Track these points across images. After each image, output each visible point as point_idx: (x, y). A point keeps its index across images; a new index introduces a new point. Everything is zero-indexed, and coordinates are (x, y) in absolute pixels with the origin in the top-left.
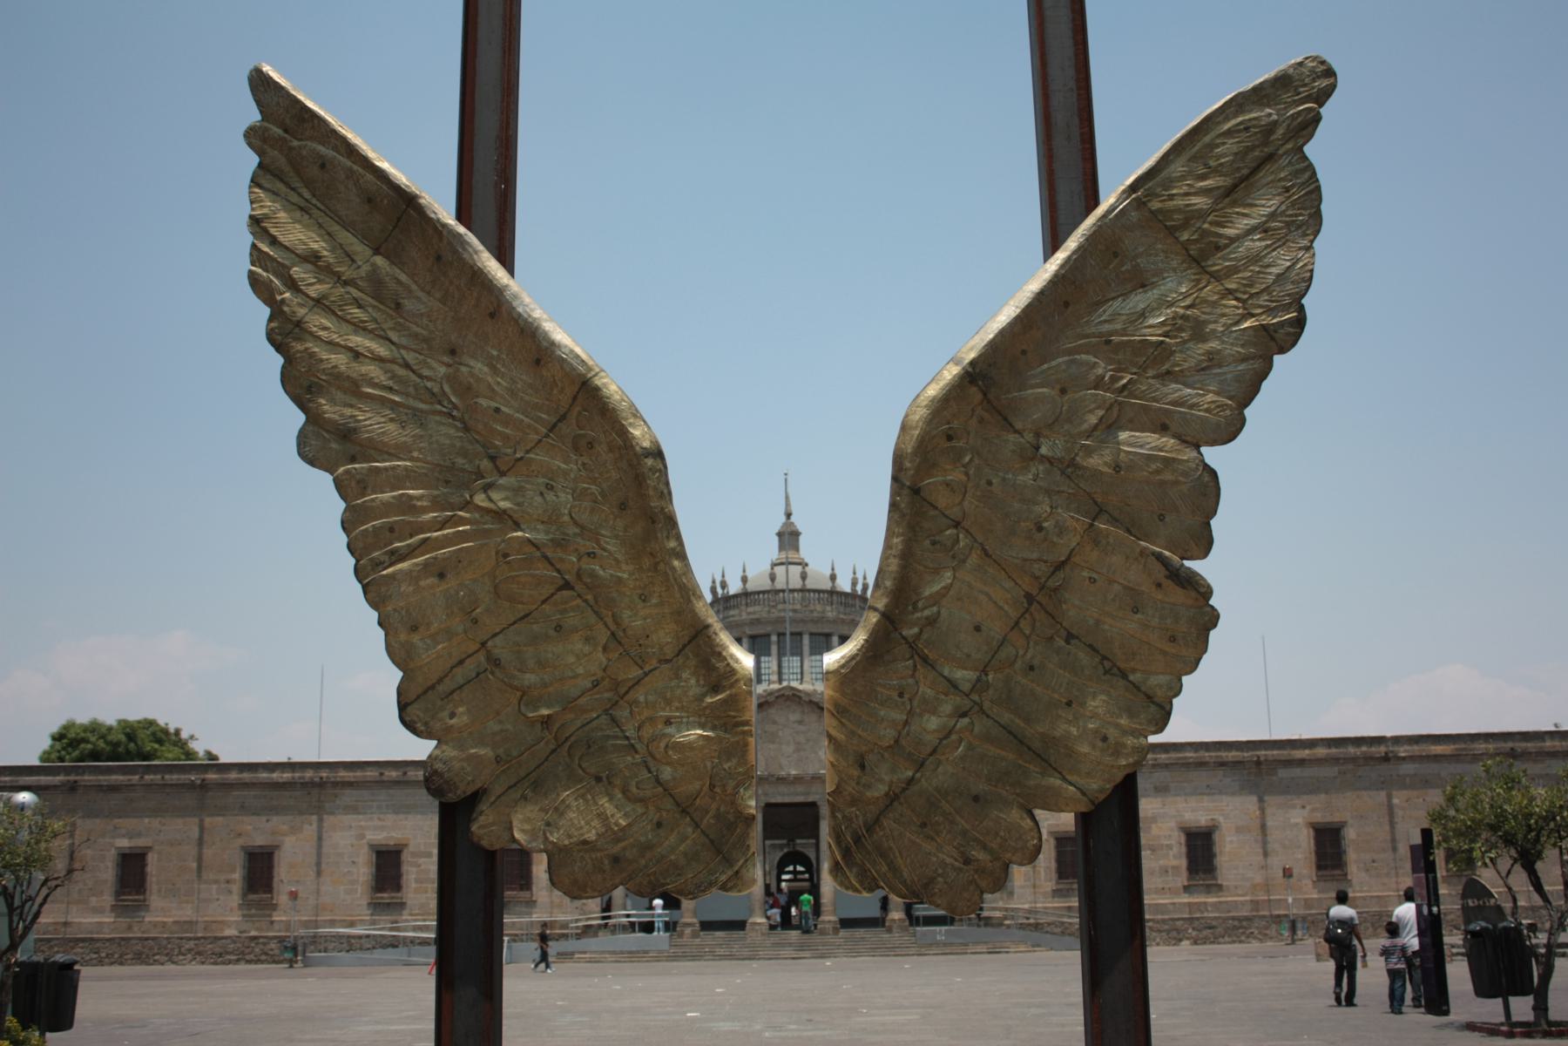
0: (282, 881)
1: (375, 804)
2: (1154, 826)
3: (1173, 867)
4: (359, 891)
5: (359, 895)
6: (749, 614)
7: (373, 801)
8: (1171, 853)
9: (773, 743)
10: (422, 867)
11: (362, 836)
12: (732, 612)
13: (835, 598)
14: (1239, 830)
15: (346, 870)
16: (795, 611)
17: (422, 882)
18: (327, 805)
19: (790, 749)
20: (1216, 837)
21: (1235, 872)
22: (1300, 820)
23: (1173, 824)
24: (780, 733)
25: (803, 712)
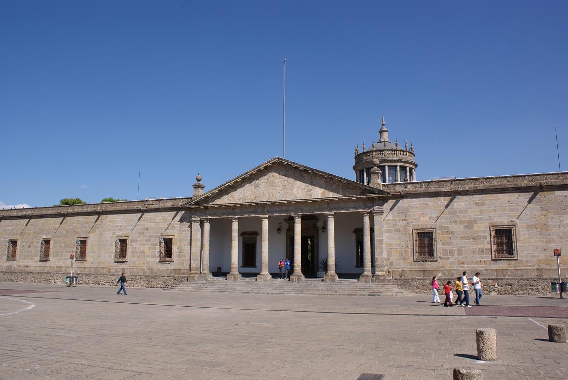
2: (475, 225)
3: (486, 249)
7: (118, 219)
8: (486, 241)
11: (114, 233)
13: (398, 151)
14: (529, 227)
16: (382, 157)
17: (133, 253)
18: (104, 221)
19: (281, 188)
20: (513, 232)
21: (526, 252)
23: (487, 224)
24: (276, 181)
25: (286, 170)
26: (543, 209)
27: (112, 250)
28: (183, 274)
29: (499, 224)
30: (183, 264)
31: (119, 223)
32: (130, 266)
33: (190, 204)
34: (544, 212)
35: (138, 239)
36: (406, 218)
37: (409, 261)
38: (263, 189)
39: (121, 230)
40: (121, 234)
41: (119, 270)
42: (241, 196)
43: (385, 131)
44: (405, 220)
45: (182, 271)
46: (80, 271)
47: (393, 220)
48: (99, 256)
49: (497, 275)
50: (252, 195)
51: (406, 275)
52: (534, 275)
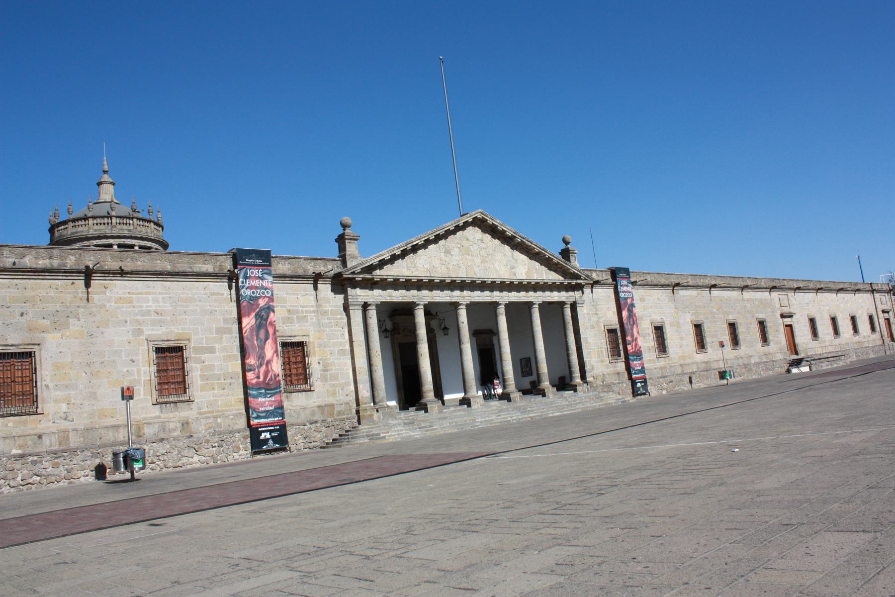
0: (47, 386)
1: (150, 297)
4: (142, 392)
5: (142, 396)
6: (96, 230)
9: (469, 255)
10: (207, 363)
11: (138, 332)
12: (80, 229)
15: (125, 370)
16: (130, 230)
22: (688, 320)
26: (676, 308)
27: (136, 377)
28: (339, 413)
29: (656, 322)
30: (334, 394)
31: (153, 307)
32: (200, 414)
33: (353, 273)
34: (676, 310)
35: (217, 346)
36: (598, 312)
37: (604, 364)
38: (457, 258)
39: (161, 323)
40: (167, 334)
41: (172, 425)
42: (427, 266)
43: (106, 183)
44: (596, 314)
45: (337, 409)
46: (20, 447)
47: (588, 314)
48: (93, 396)
49: (662, 373)
50: (443, 266)
51: (607, 380)
52: (679, 371)
